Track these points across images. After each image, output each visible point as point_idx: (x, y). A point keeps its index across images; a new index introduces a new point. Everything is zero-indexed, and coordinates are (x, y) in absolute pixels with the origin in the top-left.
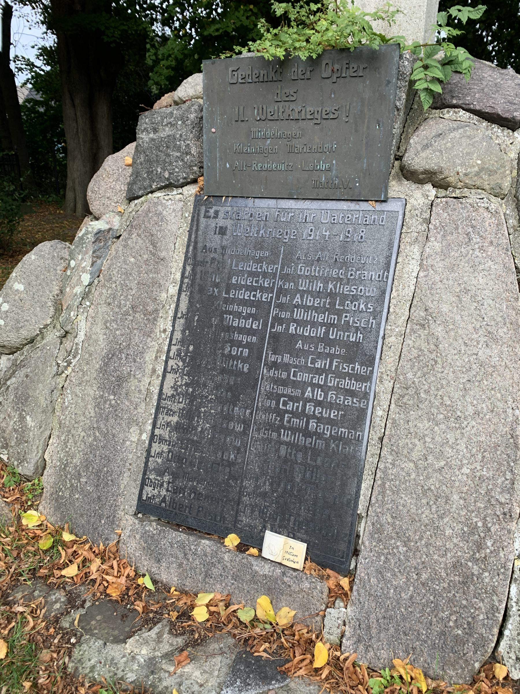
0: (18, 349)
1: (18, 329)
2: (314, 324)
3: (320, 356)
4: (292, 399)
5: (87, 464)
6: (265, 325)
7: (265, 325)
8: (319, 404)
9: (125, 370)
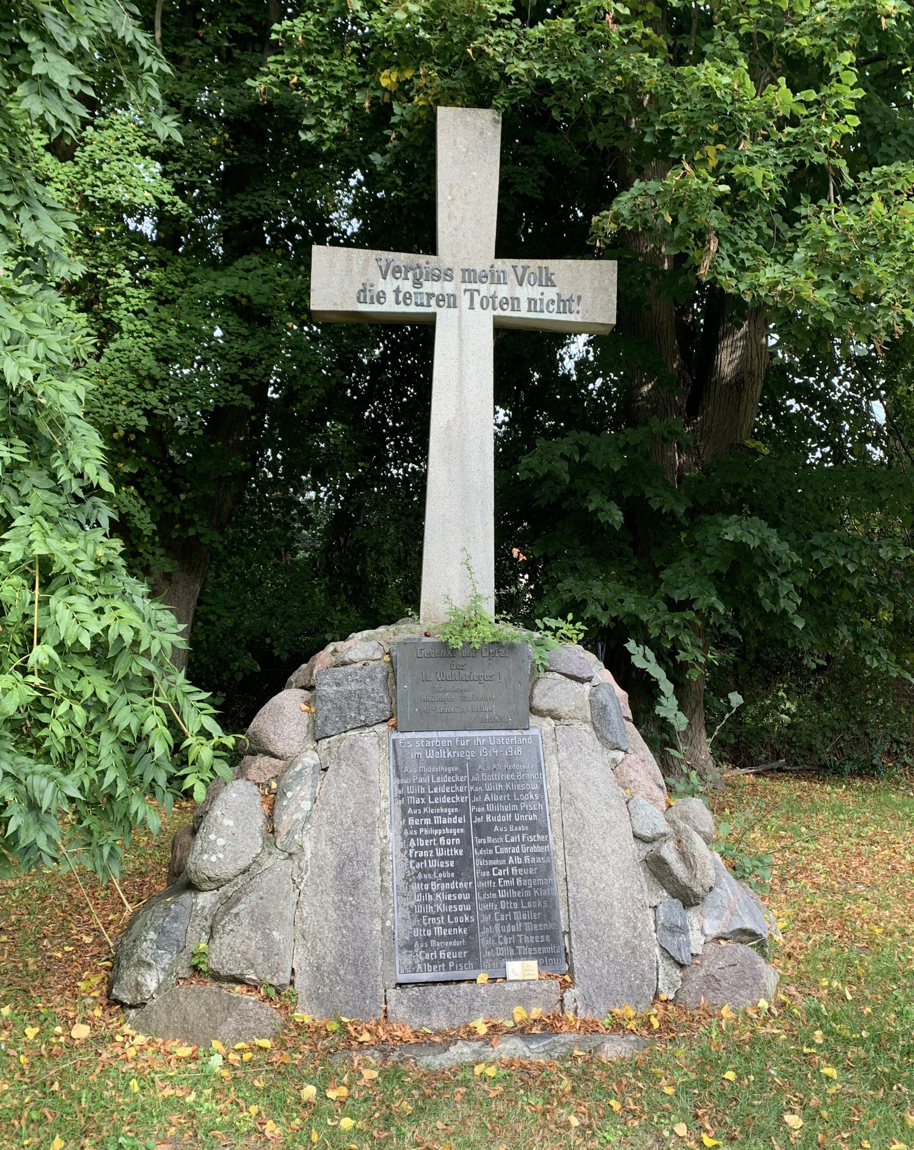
0: (230, 880)
1: (236, 861)
2: (503, 813)
3: (512, 834)
4: (502, 867)
5: (342, 959)
6: (468, 819)
7: (468, 819)
8: (519, 866)
9: (360, 873)
